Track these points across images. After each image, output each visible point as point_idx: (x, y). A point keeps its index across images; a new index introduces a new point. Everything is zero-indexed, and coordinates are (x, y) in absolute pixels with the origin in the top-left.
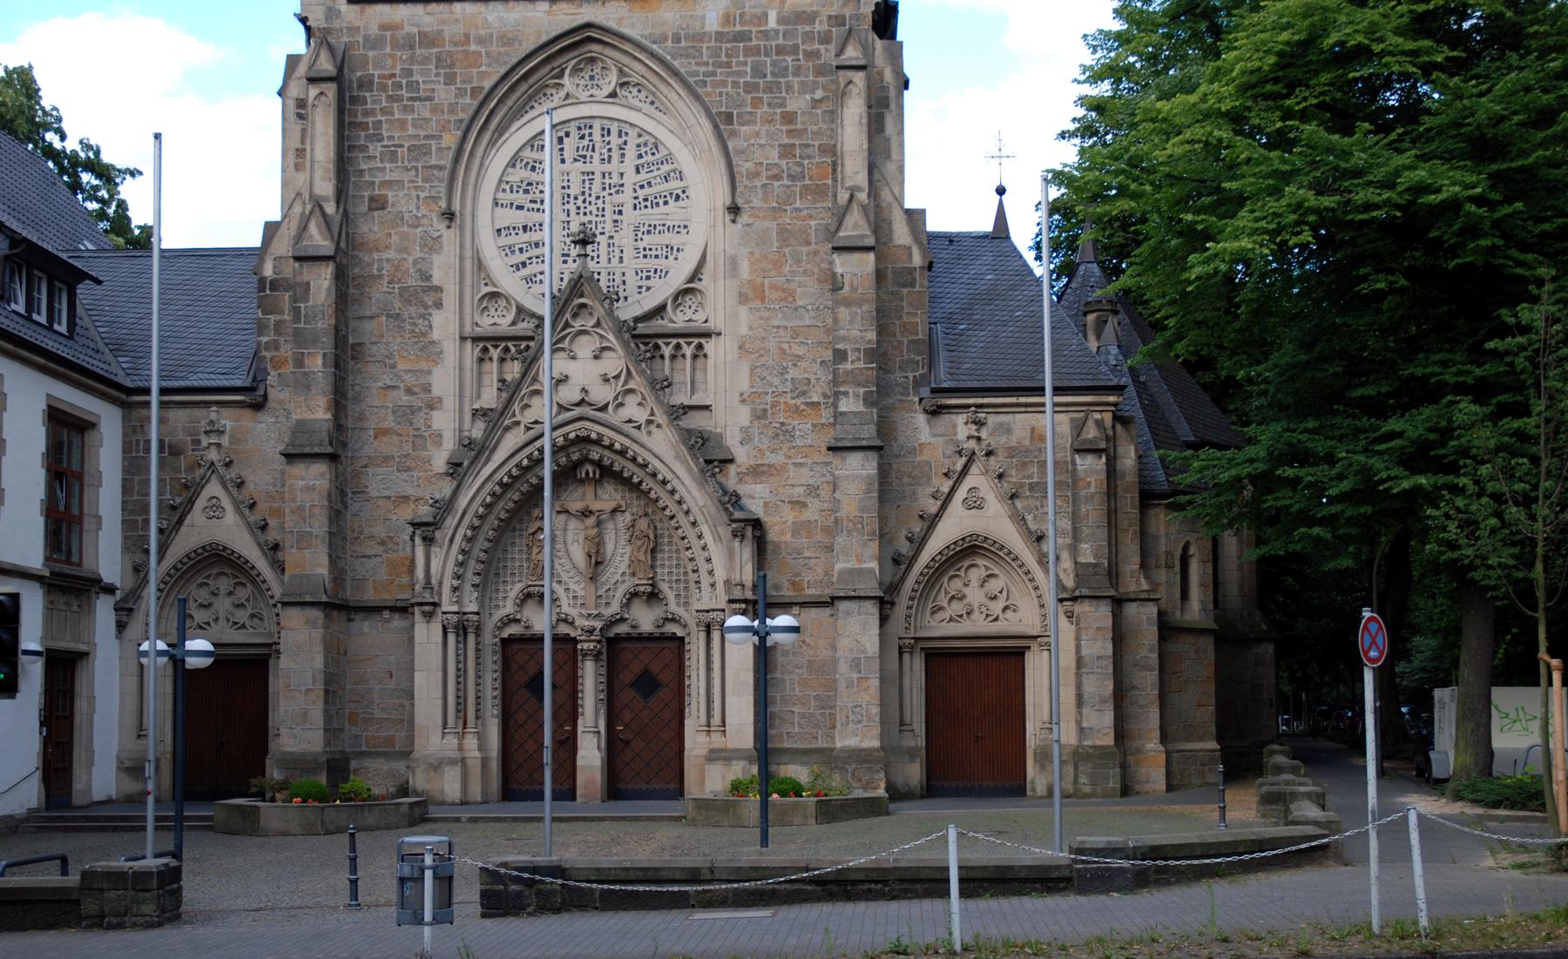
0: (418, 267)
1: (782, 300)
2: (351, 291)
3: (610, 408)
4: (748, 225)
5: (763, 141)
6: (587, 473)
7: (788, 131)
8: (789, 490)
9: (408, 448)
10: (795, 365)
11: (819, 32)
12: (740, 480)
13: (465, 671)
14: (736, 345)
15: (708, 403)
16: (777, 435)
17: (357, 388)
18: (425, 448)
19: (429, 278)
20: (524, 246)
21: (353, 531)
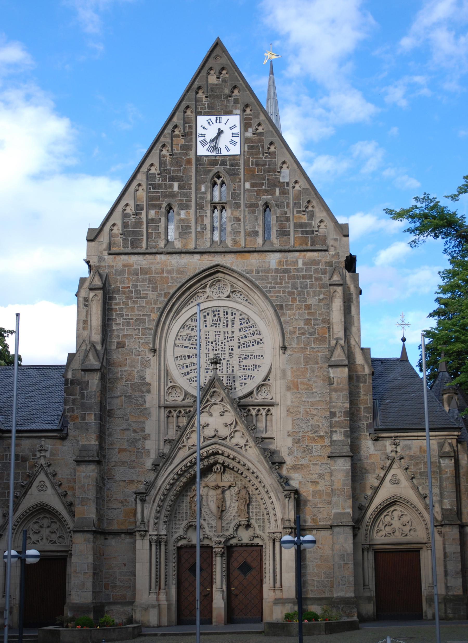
0: (139, 374)
1: (306, 389)
2: (108, 385)
3: (228, 439)
4: (290, 355)
5: (297, 318)
6: (217, 469)
7: (308, 313)
8: (310, 476)
9: (134, 458)
10: (312, 419)
11: (321, 269)
12: (288, 471)
13: (160, 563)
15: (273, 436)
16: (305, 451)
17: (110, 430)
18: (142, 457)
19: (144, 379)
20: (188, 364)
21: (108, 497)
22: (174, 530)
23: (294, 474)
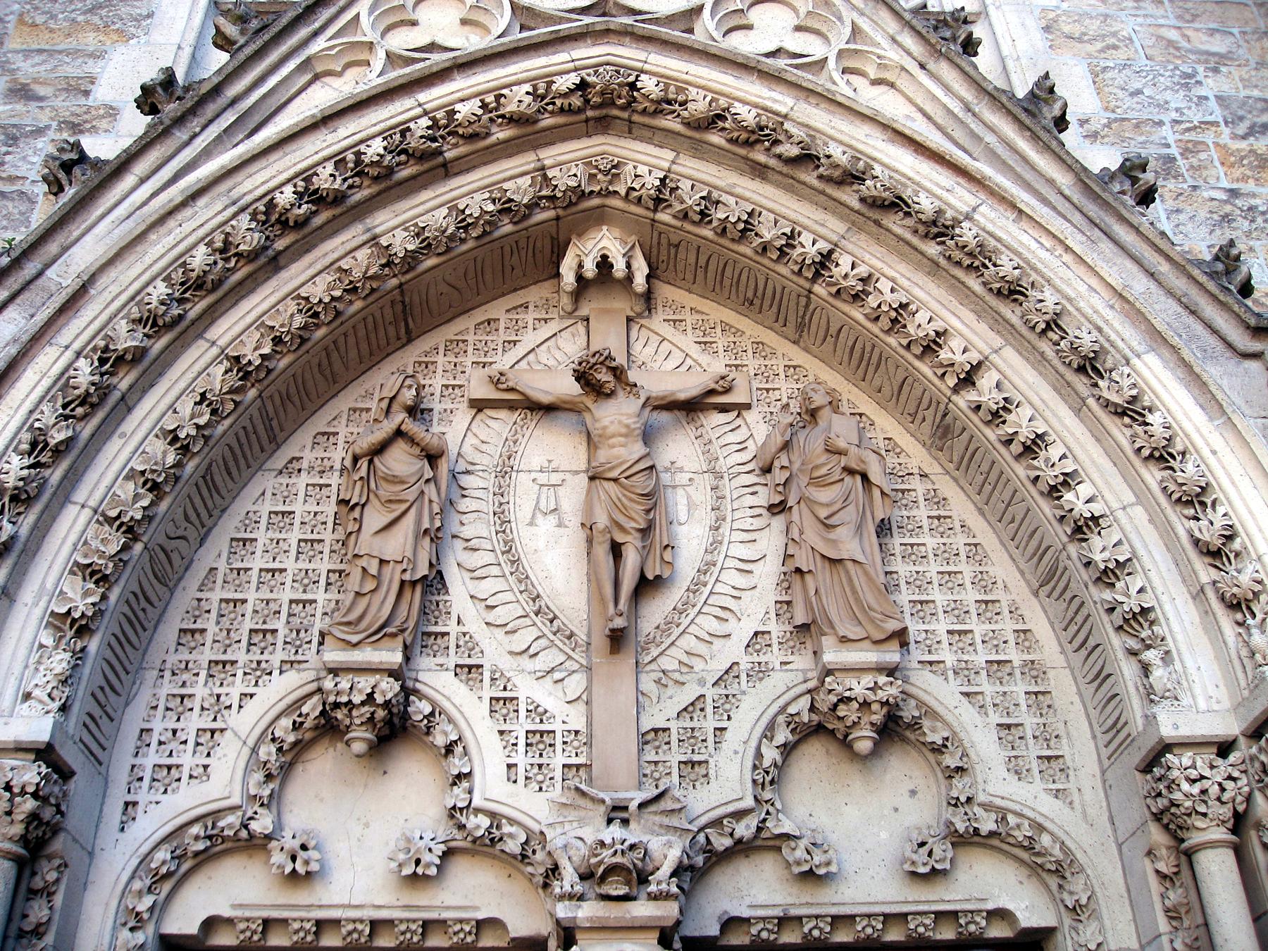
22: (152, 758)
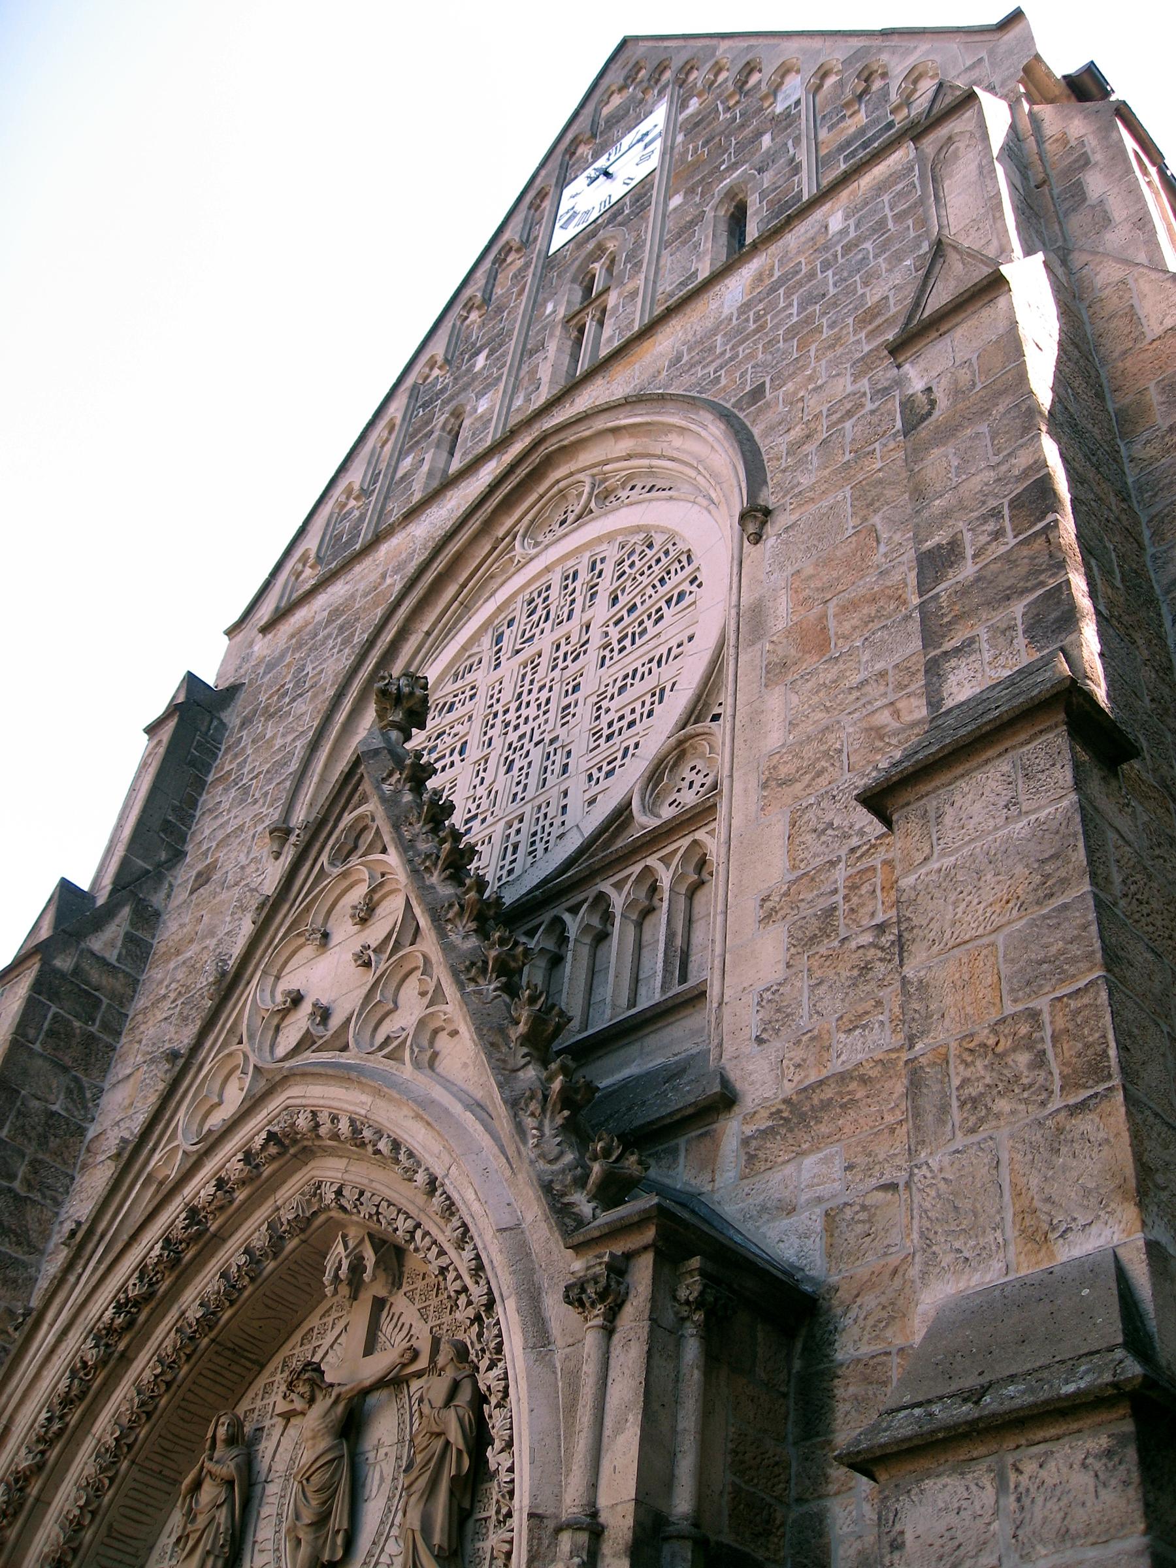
12: (751, 1158)
14: (753, 783)
16: (866, 968)
23: (789, 1169)
